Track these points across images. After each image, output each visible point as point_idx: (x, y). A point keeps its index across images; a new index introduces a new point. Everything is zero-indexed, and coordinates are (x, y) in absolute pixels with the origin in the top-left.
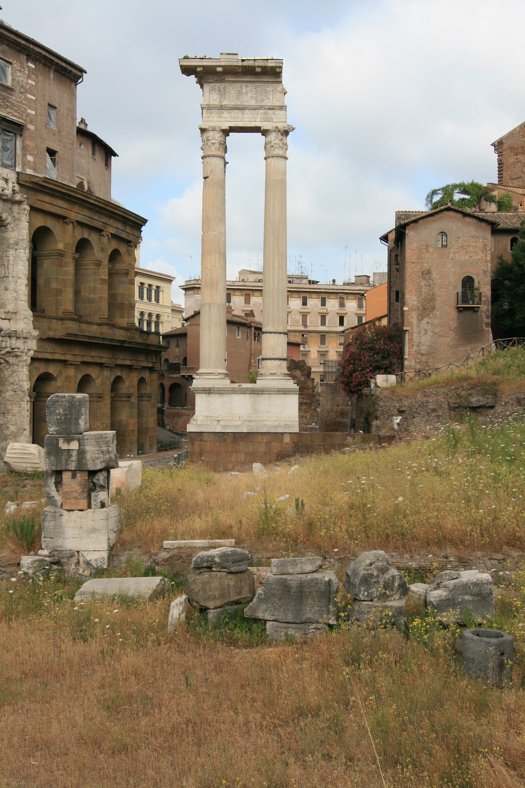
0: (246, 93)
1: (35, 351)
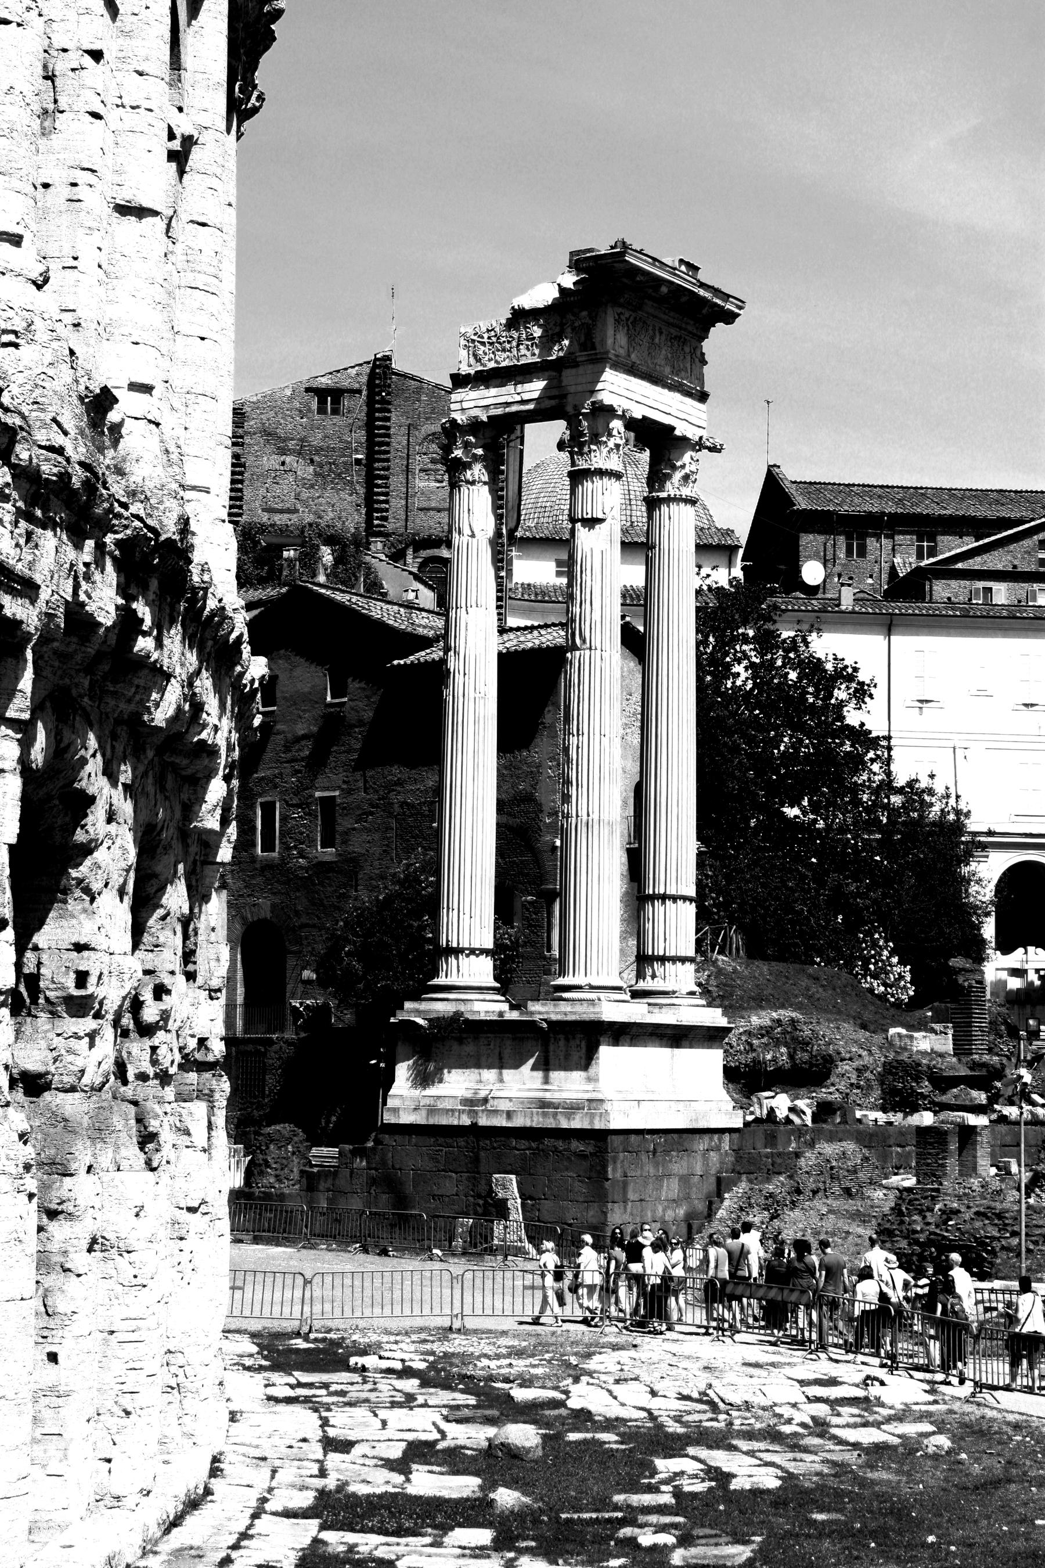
0: (660, 348)
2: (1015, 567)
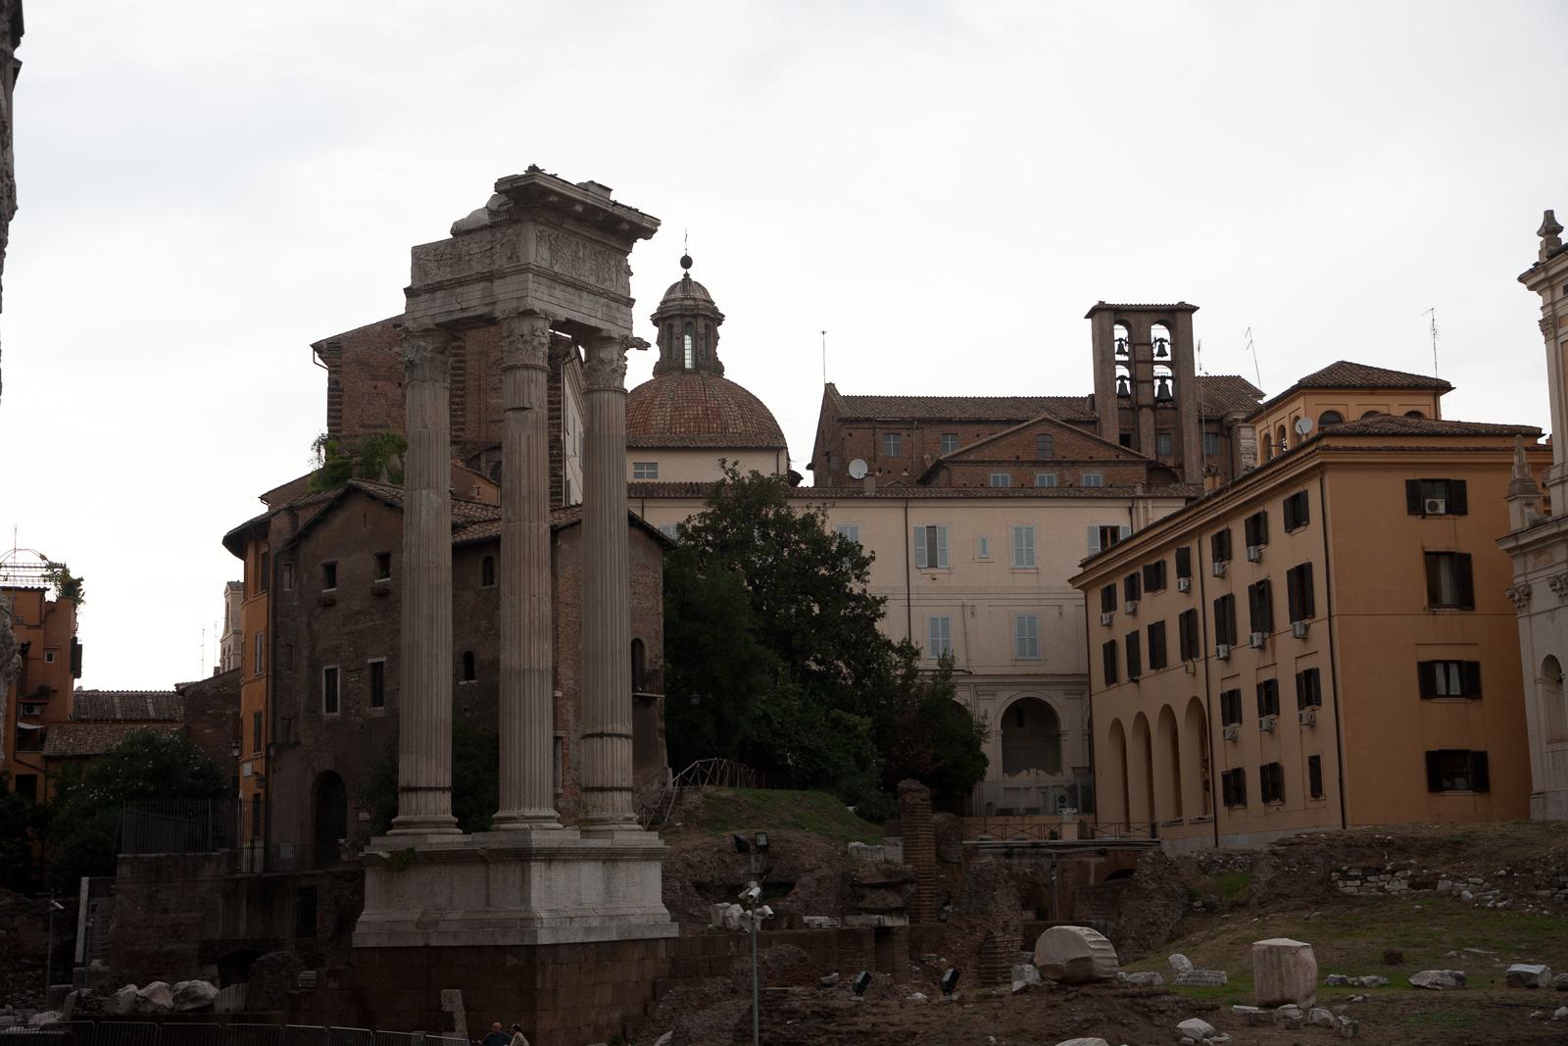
0: (585, 262)
2: (1018, 457)
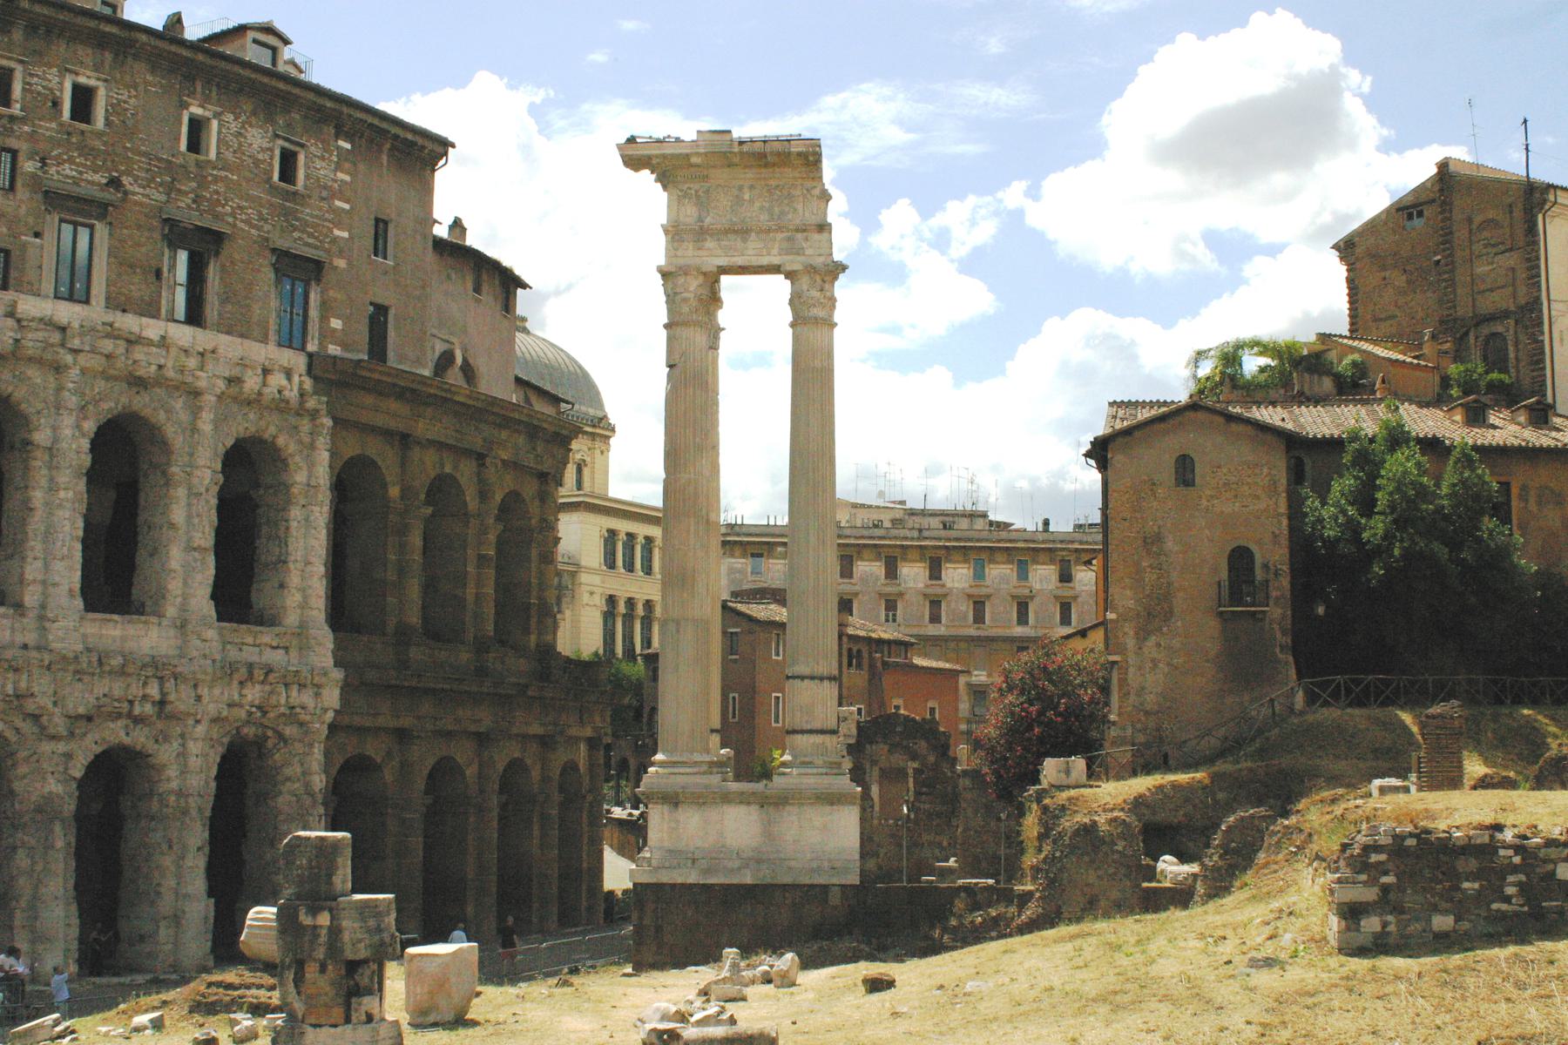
0: (751, 201)
1: (335, 711)
